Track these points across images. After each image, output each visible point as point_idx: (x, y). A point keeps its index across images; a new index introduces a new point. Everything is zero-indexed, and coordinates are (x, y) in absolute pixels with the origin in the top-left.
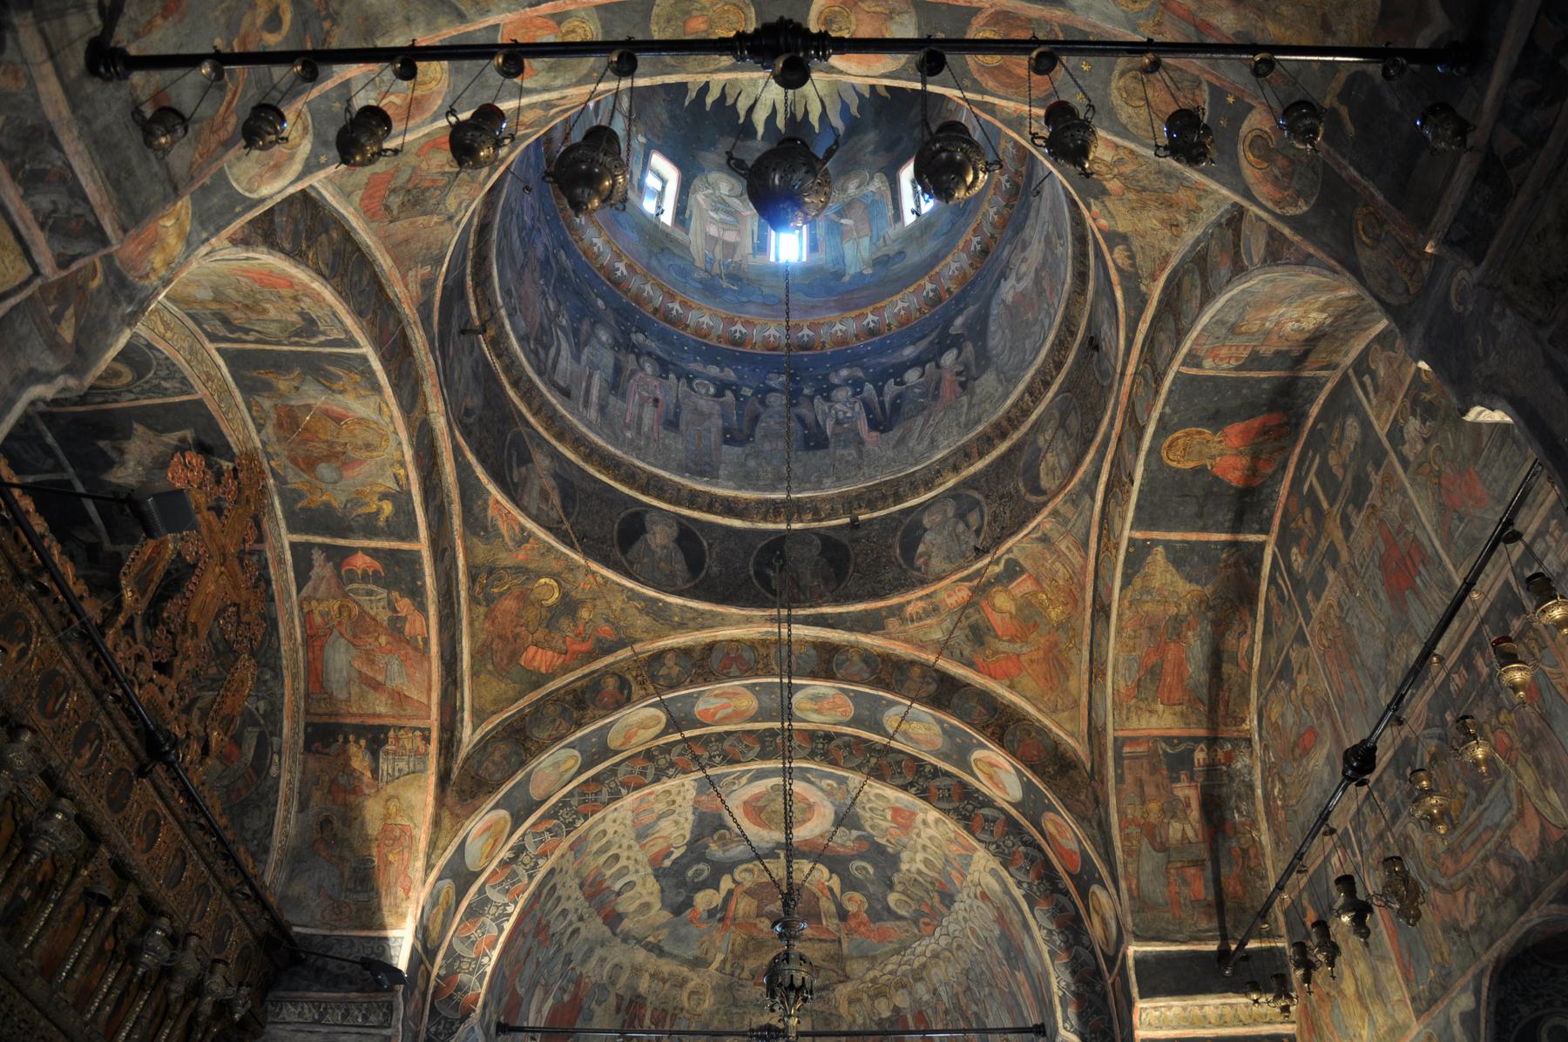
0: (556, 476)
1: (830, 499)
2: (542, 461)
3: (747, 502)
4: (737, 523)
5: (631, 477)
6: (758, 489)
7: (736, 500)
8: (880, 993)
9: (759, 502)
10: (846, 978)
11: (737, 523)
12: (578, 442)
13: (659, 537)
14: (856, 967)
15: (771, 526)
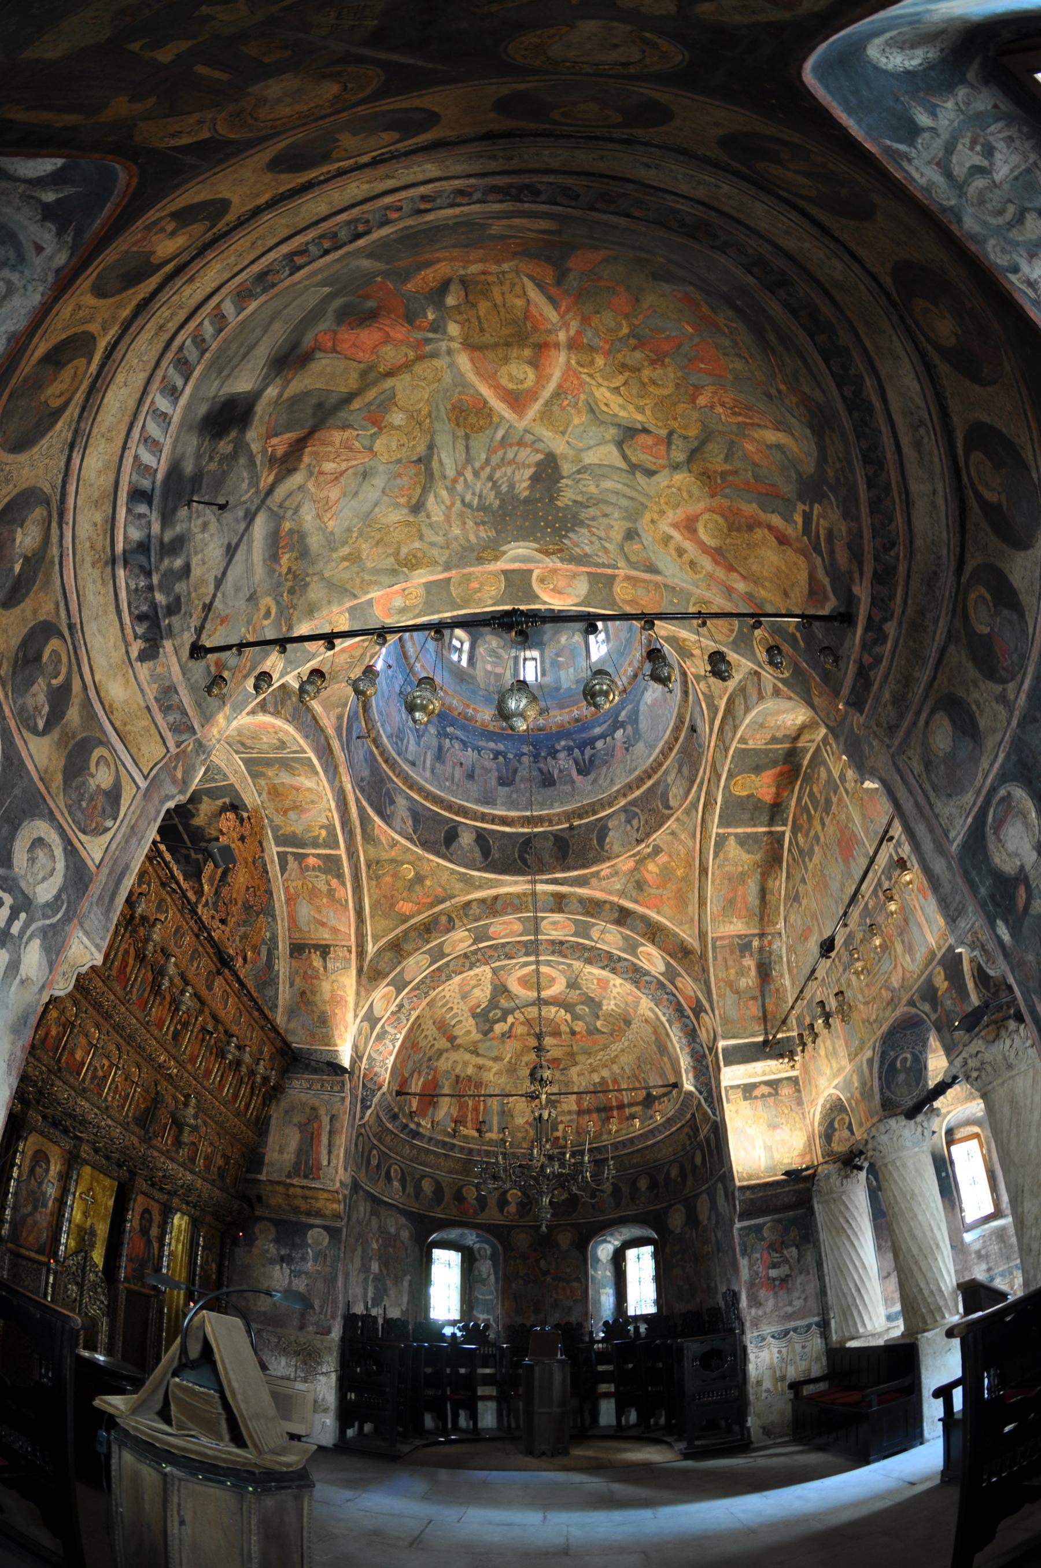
0: (409, 809)
1: (558, 814)
2: (401, 802)
3: (513, 818)
4: (508, 829)
5: (449, 807)
6: (518, 810)
7: (507, 817)
8: (593, 1071)
9: (519, 818)
10: (576, 1064)
11: (508, 829)
12: (420, 790)
13: (466, 839)
14: (581, 1058)
15: (526, 830)
